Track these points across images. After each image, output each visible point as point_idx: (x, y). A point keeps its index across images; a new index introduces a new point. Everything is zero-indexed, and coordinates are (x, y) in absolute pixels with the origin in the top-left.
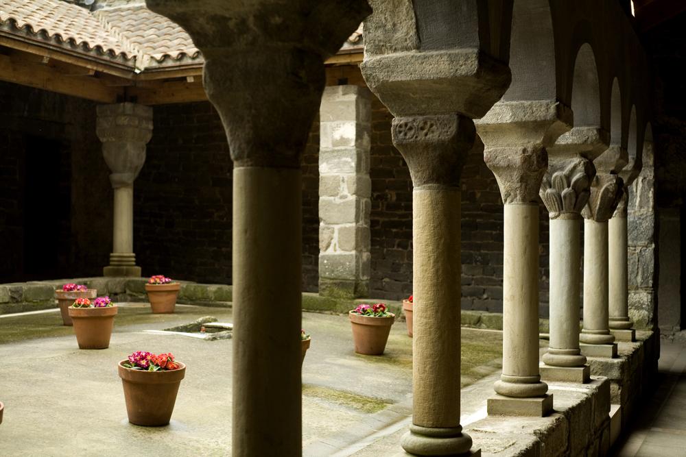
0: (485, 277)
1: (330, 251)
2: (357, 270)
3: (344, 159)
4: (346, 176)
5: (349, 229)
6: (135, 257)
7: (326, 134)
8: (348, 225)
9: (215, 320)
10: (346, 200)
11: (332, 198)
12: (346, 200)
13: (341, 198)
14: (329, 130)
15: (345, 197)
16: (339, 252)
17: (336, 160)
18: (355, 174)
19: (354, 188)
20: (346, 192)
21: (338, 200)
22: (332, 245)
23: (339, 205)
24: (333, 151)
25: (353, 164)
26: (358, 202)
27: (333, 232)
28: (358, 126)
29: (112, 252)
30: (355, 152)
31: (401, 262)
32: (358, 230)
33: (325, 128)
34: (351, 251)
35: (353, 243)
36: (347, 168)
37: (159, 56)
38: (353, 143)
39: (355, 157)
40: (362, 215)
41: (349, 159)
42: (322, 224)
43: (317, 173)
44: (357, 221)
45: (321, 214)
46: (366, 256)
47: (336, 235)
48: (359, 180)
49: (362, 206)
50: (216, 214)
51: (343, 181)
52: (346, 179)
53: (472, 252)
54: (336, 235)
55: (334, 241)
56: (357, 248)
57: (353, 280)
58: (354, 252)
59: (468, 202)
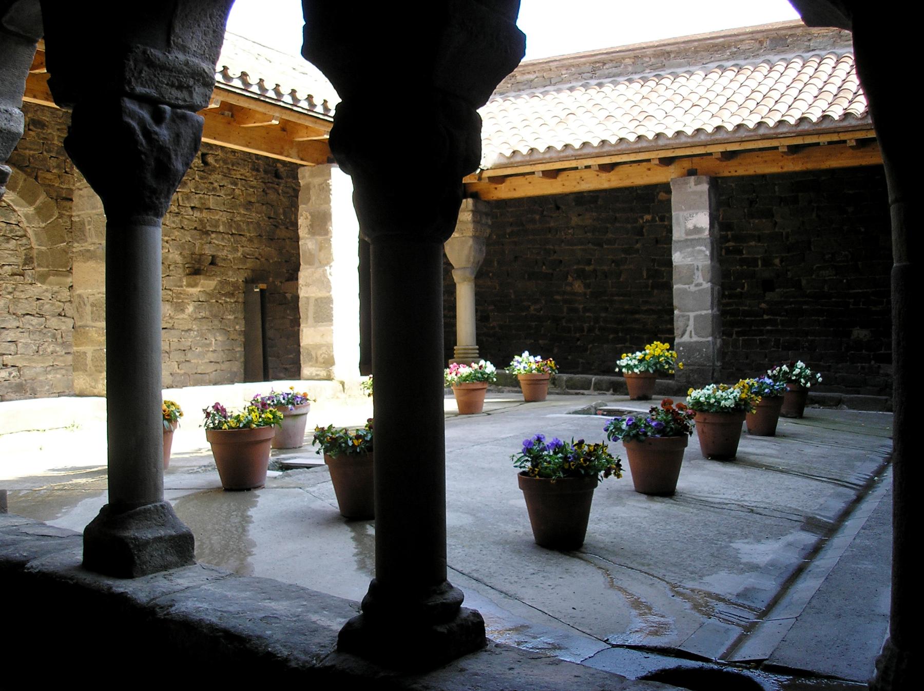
0: (812, 362)
1: (686, 338)
2: (713, 356)
3: (698, 248)
4: (700, 264)
5: (706, 316)
6: (478, 349)
7: (678, 224)
8: (704, 312)
9: (606, 405)
10: (701, 287)
11: (687, 286)
12: (701, 287)
13: (697, 285)
14: (681, 219)
15: (701, 285)
16: (695, 339)
17: (690, 250)
18: (709, 262)
19: (709, 276)
20: (701, 280)
21: (693, 288)
22: (688, 333)
23: (695, 292)
24: (686, 240)
25: (708, 253)
26: (712, 289)
27: (688, 320)
28: (711, 215)
29: (456, 345)
30: (709, 241)
31: (726, 351)
32: (713, 316)
33: (678, 219)
34: (707, 337)
35: (710, 330)
36: (701, 257)
37: (508, 153)
38: (707, 232)
39: (709, 246)
40: (715, 301)
41: (703, 248)
42: (676, 312)
43: (670, 263)
44: (712, 309)
45: (676, 302)
46: (719, 341)
47: (691, 322)
48: (713, 267)
49: (716, 293)
50: (532, 308)
51: (698, 269)
52: (700, 268)
53: (799, 338)
54: (691, 322)
55: (689, 329)
56: (713, 335)
57: (709, 366)
58: (710, 339)
59: (793, 289)
